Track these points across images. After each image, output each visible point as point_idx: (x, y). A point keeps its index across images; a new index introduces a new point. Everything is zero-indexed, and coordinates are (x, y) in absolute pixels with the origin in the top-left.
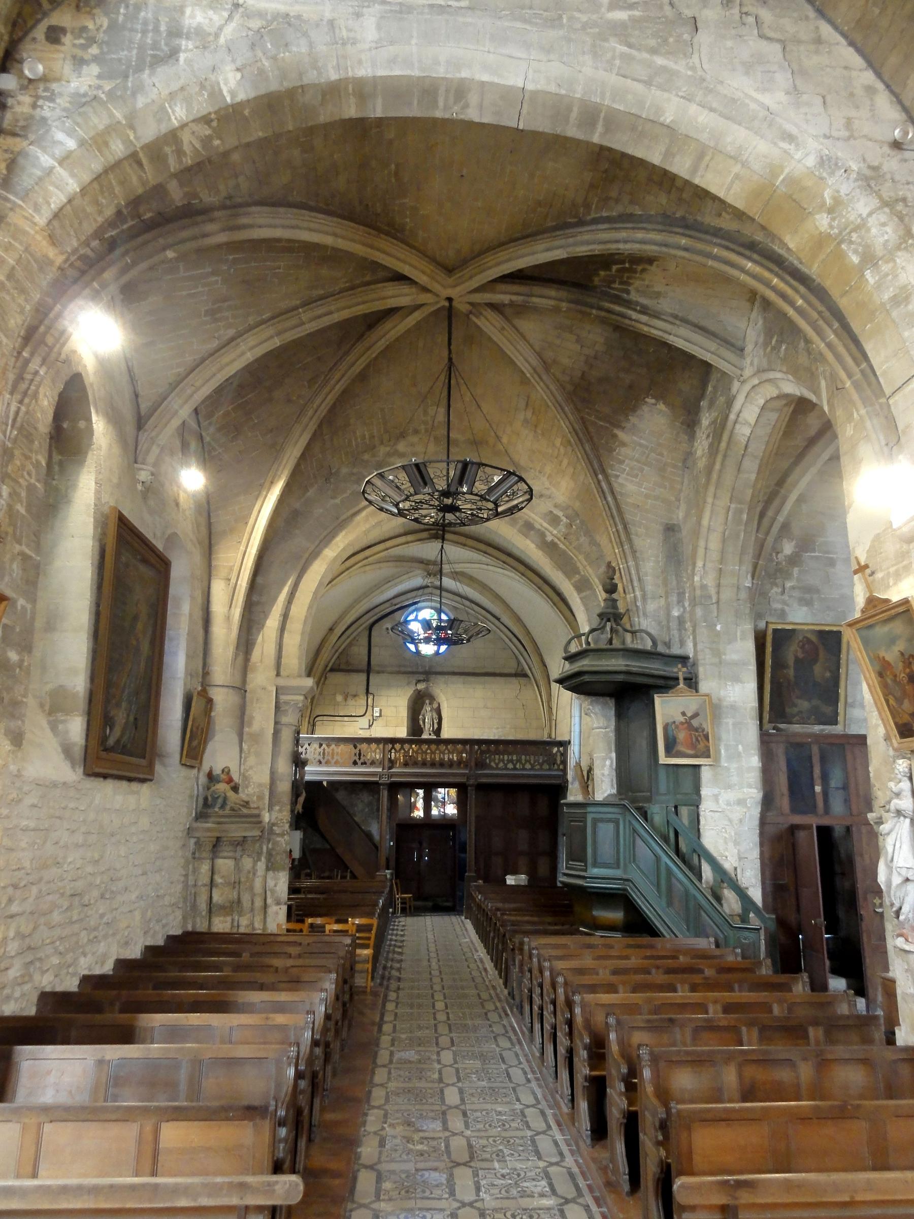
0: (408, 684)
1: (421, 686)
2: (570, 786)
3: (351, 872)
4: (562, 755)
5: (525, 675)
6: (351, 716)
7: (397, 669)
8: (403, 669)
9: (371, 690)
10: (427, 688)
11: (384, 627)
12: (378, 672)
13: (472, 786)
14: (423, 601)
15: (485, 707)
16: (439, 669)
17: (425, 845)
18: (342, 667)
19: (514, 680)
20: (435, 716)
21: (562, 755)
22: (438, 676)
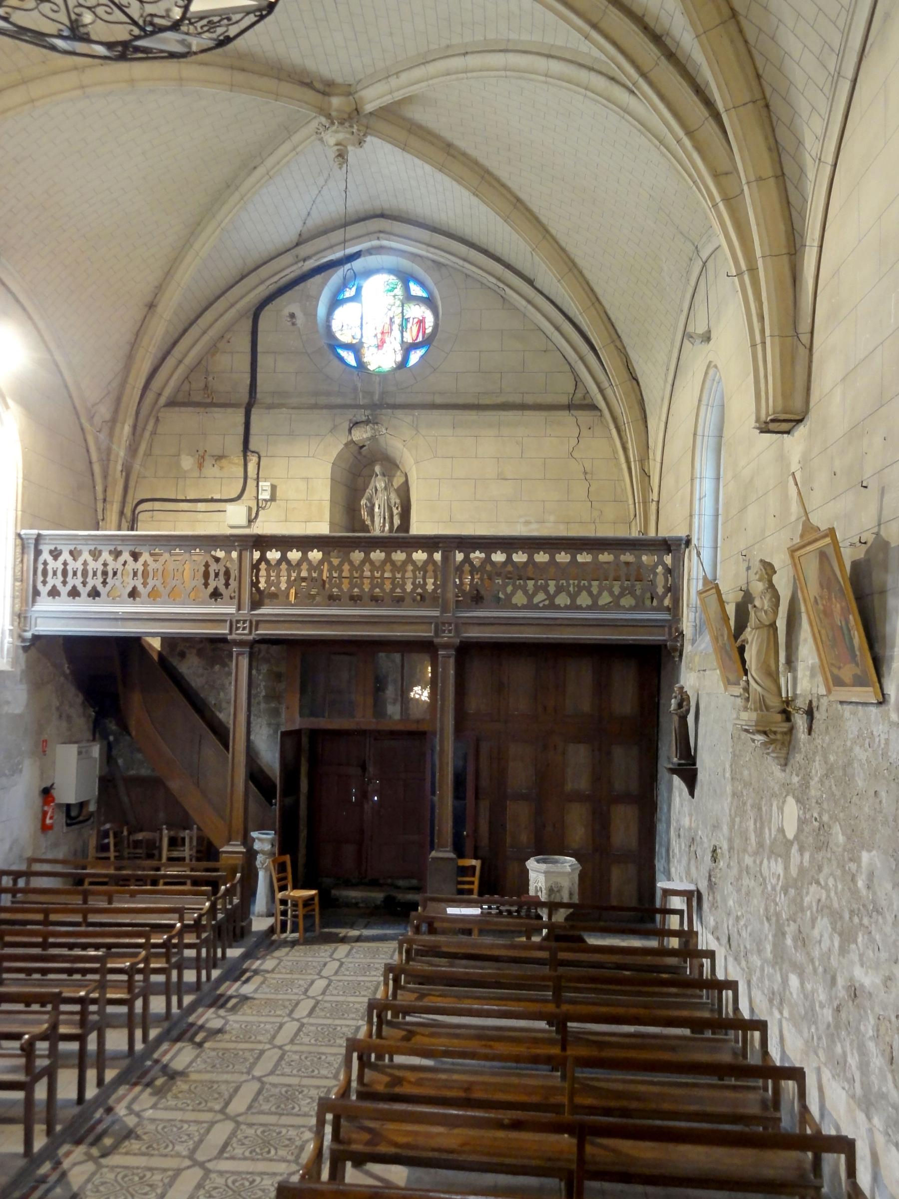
0: (334, 429)
1: (360, 435)
2: (688, 648)
3: (199, 829)
4: (669, 571)
5: (594, 407)
6: (212, 500)
7: (312, 401)
8: (323, 400)
9: (252, 446)
10: (373, 438)
11: (286, 312)
12: (270, 407)
13: (446, 646)
14: (370, 252)
15: (502, 478)
16: (400, 399)
17: (371, 769)
18: (197, 398)
19: (565, 417)
20: (395, 499)
21: (669, 571)
22: (399, 413)
